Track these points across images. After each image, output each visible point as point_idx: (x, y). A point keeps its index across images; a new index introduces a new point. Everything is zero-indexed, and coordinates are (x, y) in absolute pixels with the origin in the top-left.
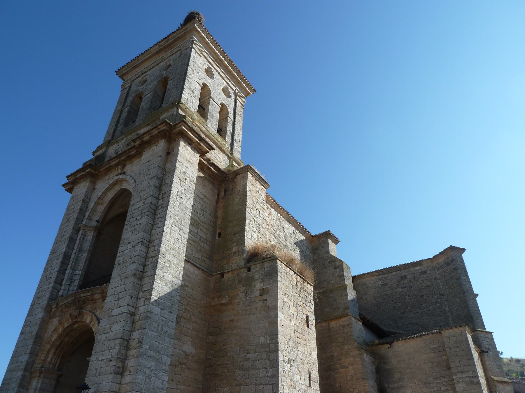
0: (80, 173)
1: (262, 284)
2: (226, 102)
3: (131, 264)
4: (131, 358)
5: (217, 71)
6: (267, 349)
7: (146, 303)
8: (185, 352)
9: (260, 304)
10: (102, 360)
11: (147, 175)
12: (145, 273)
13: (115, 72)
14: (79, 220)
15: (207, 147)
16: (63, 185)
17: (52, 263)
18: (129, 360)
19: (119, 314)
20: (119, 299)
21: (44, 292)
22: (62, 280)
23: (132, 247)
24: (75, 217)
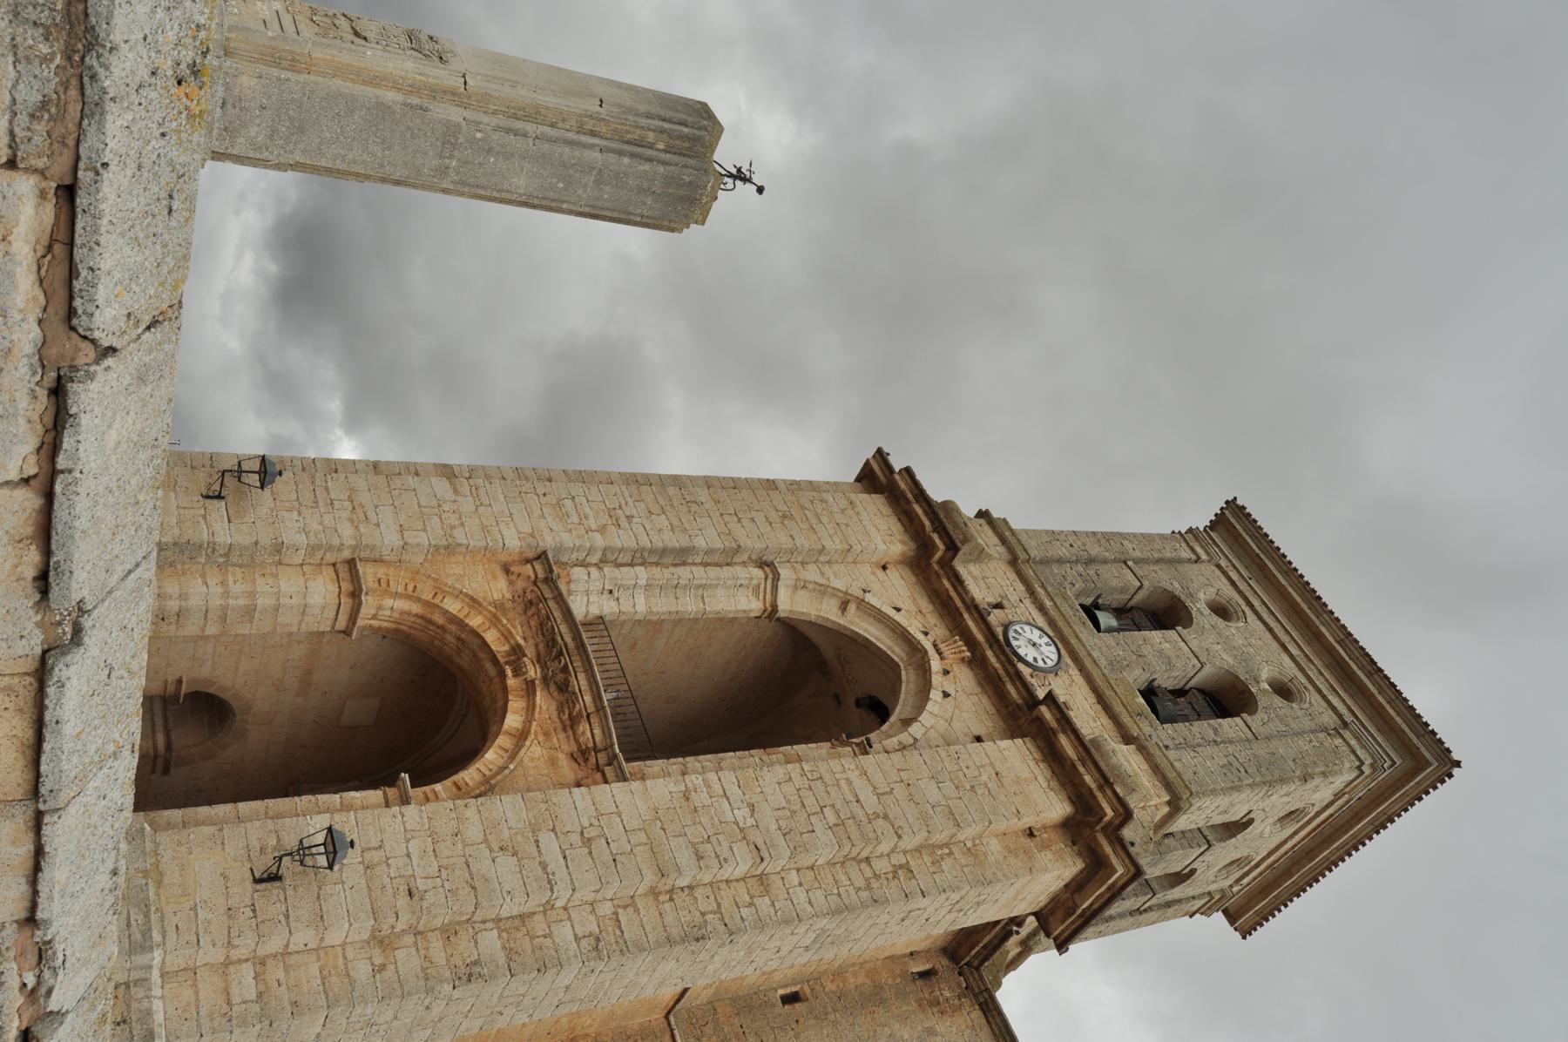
0: (925, 512)
2: (1201, 877)
3: (693, 845)
4: (422, 952)
5: (1295, 833)
7: (584, 942)
10: (408, 855)
11: (957, 787)
12: (671, 899)
13: (1235, 498)
15: (1063, 932)
16: (880, 451)
17: (660, 512)
18: (413, 950)
19: (544, 866)
20: (587, 842)
21: (575, 519)
23: (742, 830)
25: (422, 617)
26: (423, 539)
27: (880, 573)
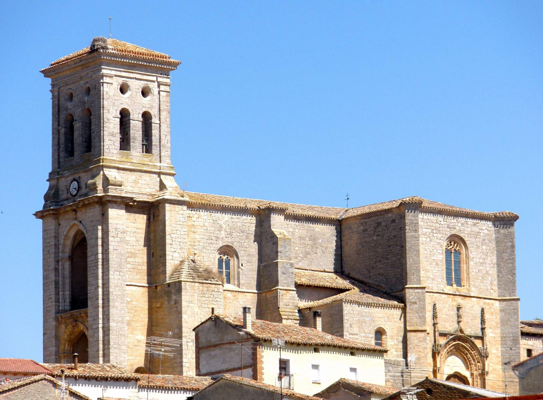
1: (175, 297)
6: (178, 336)
8: (137, 340)
9: (175, 309)
14: (57, 253)
22: (59, 299)
24: (53, 252)
25: (69, 342)
26: (54, 342)
27: (61, 226)
